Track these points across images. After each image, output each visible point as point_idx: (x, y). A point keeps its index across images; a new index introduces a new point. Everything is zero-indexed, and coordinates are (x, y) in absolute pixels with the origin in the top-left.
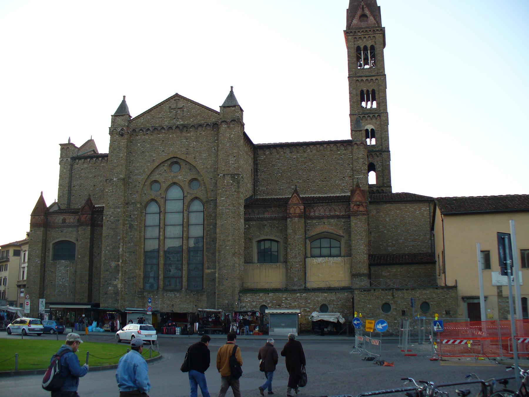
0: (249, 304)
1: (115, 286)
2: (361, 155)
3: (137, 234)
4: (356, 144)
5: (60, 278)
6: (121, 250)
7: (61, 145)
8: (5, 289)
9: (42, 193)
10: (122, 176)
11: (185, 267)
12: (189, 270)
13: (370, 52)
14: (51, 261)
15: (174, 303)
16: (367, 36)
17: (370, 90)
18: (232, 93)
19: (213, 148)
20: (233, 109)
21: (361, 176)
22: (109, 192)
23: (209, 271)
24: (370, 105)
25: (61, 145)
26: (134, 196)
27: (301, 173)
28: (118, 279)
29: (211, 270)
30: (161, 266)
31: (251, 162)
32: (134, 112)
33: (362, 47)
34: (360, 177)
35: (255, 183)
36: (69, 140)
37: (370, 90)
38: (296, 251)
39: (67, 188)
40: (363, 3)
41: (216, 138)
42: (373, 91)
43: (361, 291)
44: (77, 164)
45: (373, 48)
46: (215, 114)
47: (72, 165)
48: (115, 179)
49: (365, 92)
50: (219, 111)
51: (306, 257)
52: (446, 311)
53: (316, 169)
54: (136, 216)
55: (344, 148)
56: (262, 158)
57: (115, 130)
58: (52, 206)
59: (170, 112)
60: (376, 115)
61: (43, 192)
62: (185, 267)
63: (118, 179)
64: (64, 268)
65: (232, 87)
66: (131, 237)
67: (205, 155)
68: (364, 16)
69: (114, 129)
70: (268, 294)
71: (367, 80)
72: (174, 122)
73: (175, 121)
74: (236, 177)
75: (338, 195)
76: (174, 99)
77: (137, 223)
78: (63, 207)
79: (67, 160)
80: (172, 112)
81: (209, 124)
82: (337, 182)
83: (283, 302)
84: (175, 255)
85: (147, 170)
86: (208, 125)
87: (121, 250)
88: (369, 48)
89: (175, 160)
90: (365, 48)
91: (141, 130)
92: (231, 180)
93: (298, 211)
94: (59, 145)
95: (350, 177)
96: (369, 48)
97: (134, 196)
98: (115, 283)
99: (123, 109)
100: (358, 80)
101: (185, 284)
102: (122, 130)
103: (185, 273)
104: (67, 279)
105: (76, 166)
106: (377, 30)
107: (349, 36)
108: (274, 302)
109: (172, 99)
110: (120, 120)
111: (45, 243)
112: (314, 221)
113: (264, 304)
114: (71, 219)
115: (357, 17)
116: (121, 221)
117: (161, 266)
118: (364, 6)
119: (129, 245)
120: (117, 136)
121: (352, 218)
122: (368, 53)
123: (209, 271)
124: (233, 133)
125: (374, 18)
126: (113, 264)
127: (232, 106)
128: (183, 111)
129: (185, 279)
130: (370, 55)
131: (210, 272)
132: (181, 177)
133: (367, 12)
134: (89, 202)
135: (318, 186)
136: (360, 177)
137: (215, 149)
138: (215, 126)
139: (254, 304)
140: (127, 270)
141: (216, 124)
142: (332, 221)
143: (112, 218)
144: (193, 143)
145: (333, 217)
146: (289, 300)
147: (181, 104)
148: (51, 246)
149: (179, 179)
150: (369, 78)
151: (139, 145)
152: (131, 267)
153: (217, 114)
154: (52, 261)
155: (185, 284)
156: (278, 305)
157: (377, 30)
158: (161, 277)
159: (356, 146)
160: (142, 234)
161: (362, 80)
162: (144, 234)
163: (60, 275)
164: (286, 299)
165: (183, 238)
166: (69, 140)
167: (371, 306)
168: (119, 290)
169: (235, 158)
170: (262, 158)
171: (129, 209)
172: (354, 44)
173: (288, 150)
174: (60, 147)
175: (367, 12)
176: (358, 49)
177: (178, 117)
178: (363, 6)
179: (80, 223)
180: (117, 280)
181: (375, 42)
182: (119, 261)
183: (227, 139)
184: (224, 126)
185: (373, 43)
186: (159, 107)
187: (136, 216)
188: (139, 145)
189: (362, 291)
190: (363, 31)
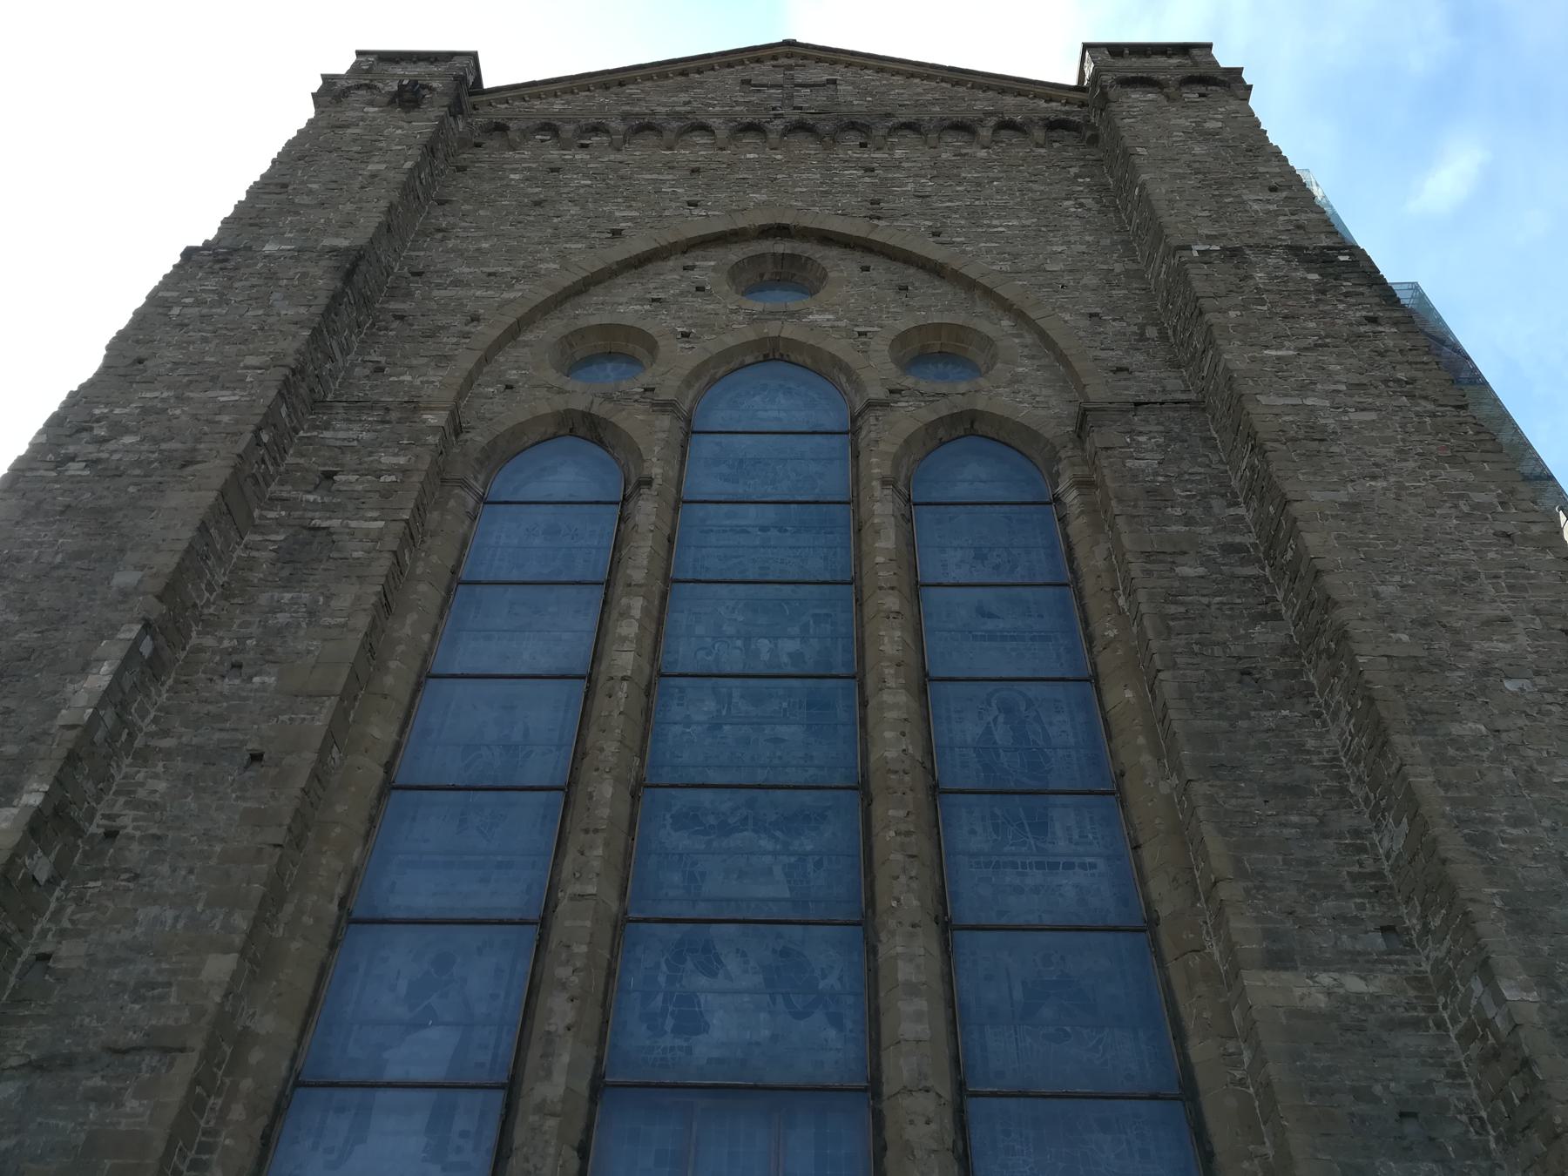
3: (358, 598)
26: (407, 378)
29: (1325, 979)
66: (282, 618)
84: (765, 843)
116: (216, 470)
119: (226, 685)
131: (1322, 1001)
140: (69, 954)
149: (813, 326)
152: (146, 913)
160: (408, 627)
162: (426, 637)
165: (858, 677)
171: (327, 434)
186: (680, 79)
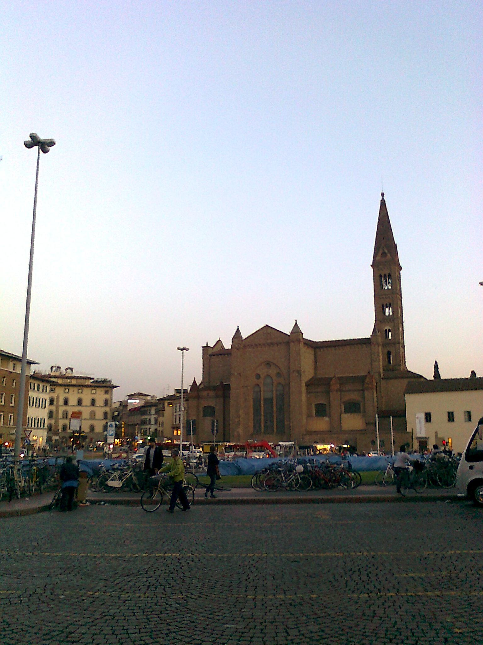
1: (238, 432)
4: (373, 344)
9: (195, 378)
12: (277, 422)
18: (296, 323)
24: (388, 312)
30: (262, 420)
31: (312, 357)
33: (383, 275)
35: (316, 369)
36: (207, 344)
42: (390, 304)
47: (210, 360)
51: (341, 413)
58: (200, 385)
68: (384, 254)
78: (206, 385)
89: (268, 362)
93: (336, 388)
98: (238, 430)
101: (275, 430)
103: (275, 424)
105: (212, 360)
111: (198, 407)
114: (212, 393)
115: (380, 254)
117: (262, 420)
126: (237, 420)
134: (222, 383)
138: (288, 343)
145: (355, 390)
147: (269, 331)
148: (201, 409)
155: (275, 430)
158: (263, 426)
159: (373, 346)
161: (383, 297)
166: (207, 344)
173: (333, 349)
176: (381, 276)
179: (217, 396)
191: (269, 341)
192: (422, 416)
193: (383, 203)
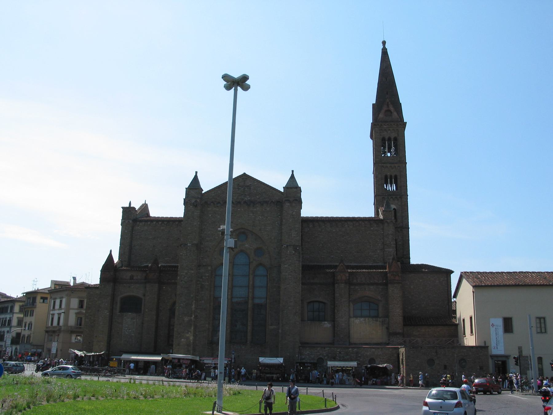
0: (308, 357)
2: (391, 232)
4: (387, 222)
5: (126, 329)
6: (194, 306)
7: (123, 208)
8: (31, 333)
9: (111, 251)
10: (195, 242)
11: (250, 323)
13: (393, 143)
14: (118, 313)
15: (240, 354)
16: (391, 129)
17: (393, 175)
19: (277, 223)
20: (295, 190)
21: (391, 250)
22: (184, 255)
23: (272, 327)
25: (123, 208)
27: (339, 245)
28: (190, 332)
32: (206, 186)
33: (387, 138)
34: (389, 250)
37: (393, 175)
38: (343, 312)
39: (128, 247)
40: (388, 100)
41: (279, 214)
43: (411, 348)
44: (138, 226)
45: (396, 139)
46: (278, 193)
47: (133, 227)
48: (189, 244)
49: (389, 177)
50: (283, 191)
51: (350, 317)
52: (480, 367)
53: (352, 242)
54: (207, 277)
55: (376, 225)
56: (306, 230)
57: (189, 201)
59: (239, 189)
60: (398, 197)
61: (112, 250)
62: (250, 323)
63: (192, 245)
64: (130, 319)
65: (293, 171)
67: (269, 228)
69: (188, 201)
70: (325, 348)
71: (391, 166)
72: (242, 197)
73: (244, 197)
74: (298, 248)
75: (371, 264)
76: (242, 178)
77: (208, 284)
79: (129, 222)
80: (240, 189)
81: (274, 201)
82: (370, 253)
83: (338, 355)
85: (217, 238)
86: (272, 202)
87: (194, 306)
88: (392, 140)
90: (389, 139)
91: (212, 202)
92: (294, 251)
94: (122, 208)
95: (381, 250)
96: (392, 140)
97: (205, 260)
98: (188, 335)
99: (195, 183)
100: (383, 166)
101: (249, 338)
102: (196, 201)
103: (249, 328)
104: (133, 330)
106: (400, 124)
107: (376, 128)
108: (329, 355)
109: (240, 177)
110: (193, 193)
112: (357, 287)
113: (321, 356)
115: (383, 111)
118: (389, 103)
120: (191, 207)
121: (389, 285)
122: (391, 143)
123: (272, 327)
124: (295, 210)
125: (397, 113)
126: (186, 319)
127: (294, 188)
128: (250, 189)
129: (249, 334)
130: (393, 145)
132: (248, 245)
133: (392, 108)
135: (354, 256)
136: (389, 250)
137: (278, 223)
139: (312, 356)
141: (279, 202)
142: (372, 287)
143: (186, 278)
144: (259, 217)
145: (372, 284)
146: (342, 354)
147: (248, 183)
148: (118, 300)
150: (393, 165)
151: (210, 215)
153: (280, 193)
154: (119, 313)
155: (249, 338)
156: (333, 358)
157: (400, 124)
159: (386, 224)
163: (127, 326)
164: (340, 353)
167: (418, 361)
168: (192, 341)
169: (297, 232)
170: (306, 230)
172: (380, 135)
174: (122, 209)
175: (392, 109)
176: (383, 140)
177: (246, 194)
178: (388, 103)
180: (189, 333)
181: (398, 134)
182: (191, 316)
183: (289, 216)
184: (288, 204)
185: (396, 135)
187: (207, 277)
188: (210, 215)
189: (412, 348)
190: (388, 125)
191: (247, 198)
192: (499, 322)
193: (385, 53)
